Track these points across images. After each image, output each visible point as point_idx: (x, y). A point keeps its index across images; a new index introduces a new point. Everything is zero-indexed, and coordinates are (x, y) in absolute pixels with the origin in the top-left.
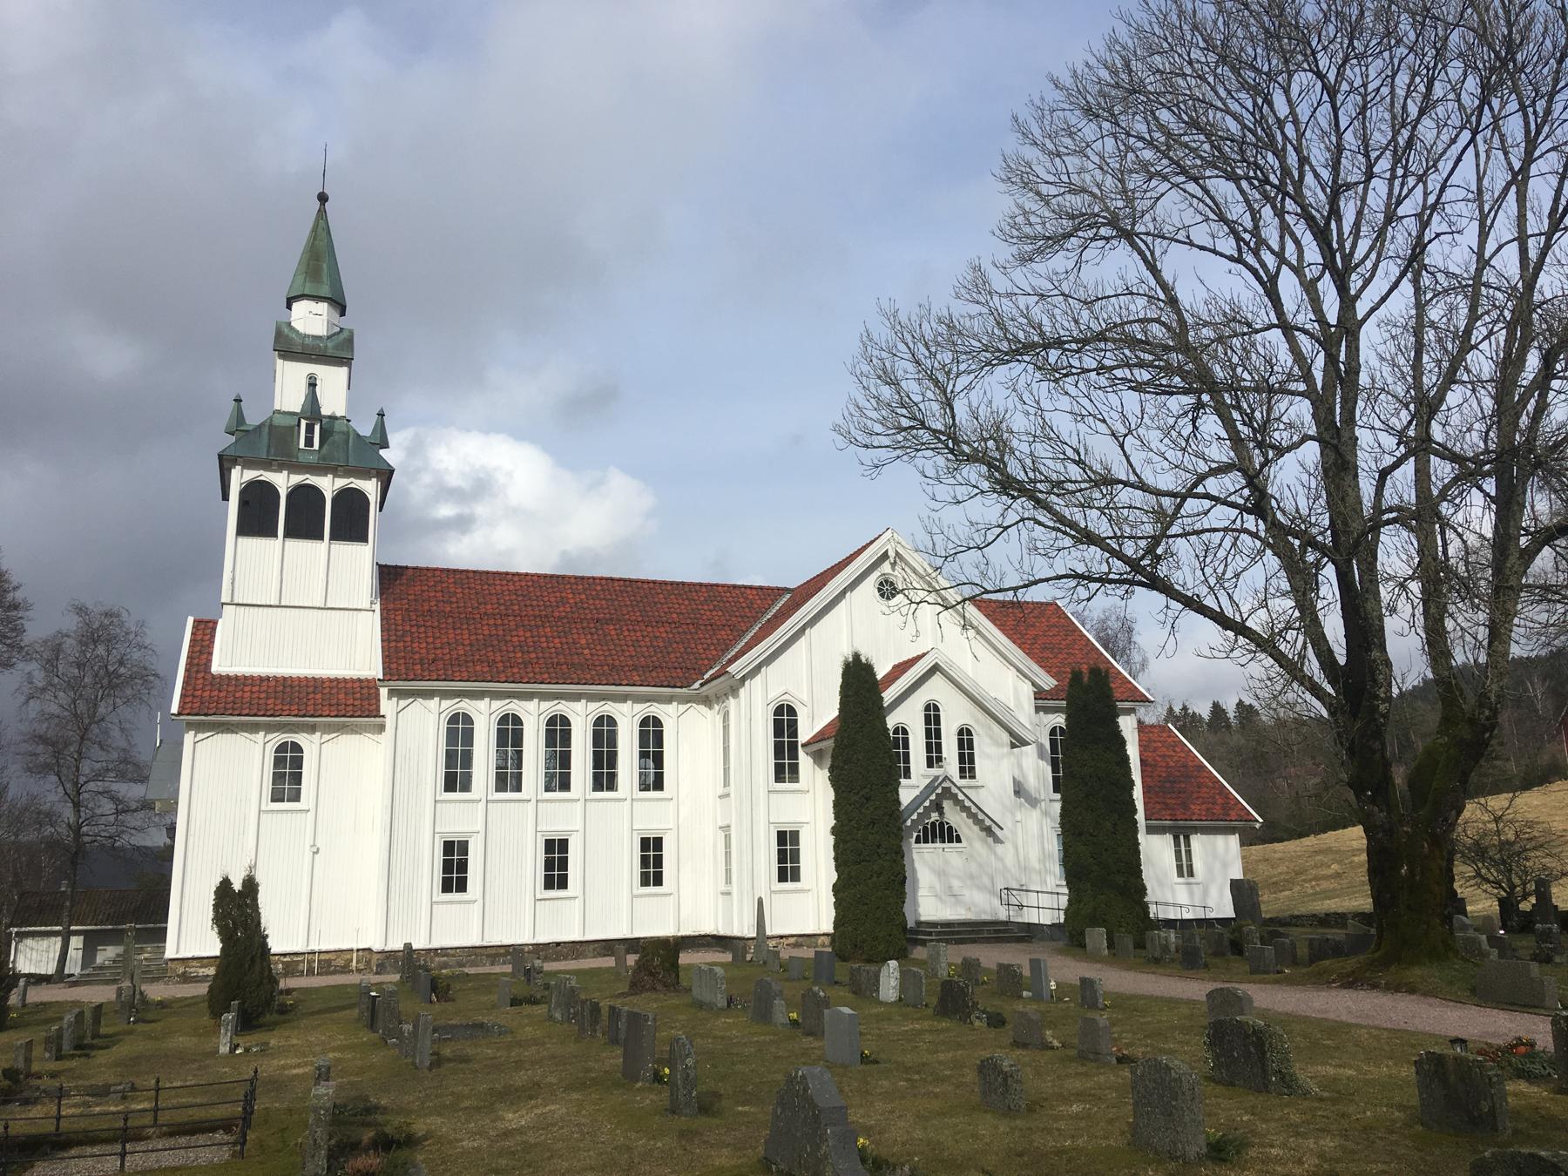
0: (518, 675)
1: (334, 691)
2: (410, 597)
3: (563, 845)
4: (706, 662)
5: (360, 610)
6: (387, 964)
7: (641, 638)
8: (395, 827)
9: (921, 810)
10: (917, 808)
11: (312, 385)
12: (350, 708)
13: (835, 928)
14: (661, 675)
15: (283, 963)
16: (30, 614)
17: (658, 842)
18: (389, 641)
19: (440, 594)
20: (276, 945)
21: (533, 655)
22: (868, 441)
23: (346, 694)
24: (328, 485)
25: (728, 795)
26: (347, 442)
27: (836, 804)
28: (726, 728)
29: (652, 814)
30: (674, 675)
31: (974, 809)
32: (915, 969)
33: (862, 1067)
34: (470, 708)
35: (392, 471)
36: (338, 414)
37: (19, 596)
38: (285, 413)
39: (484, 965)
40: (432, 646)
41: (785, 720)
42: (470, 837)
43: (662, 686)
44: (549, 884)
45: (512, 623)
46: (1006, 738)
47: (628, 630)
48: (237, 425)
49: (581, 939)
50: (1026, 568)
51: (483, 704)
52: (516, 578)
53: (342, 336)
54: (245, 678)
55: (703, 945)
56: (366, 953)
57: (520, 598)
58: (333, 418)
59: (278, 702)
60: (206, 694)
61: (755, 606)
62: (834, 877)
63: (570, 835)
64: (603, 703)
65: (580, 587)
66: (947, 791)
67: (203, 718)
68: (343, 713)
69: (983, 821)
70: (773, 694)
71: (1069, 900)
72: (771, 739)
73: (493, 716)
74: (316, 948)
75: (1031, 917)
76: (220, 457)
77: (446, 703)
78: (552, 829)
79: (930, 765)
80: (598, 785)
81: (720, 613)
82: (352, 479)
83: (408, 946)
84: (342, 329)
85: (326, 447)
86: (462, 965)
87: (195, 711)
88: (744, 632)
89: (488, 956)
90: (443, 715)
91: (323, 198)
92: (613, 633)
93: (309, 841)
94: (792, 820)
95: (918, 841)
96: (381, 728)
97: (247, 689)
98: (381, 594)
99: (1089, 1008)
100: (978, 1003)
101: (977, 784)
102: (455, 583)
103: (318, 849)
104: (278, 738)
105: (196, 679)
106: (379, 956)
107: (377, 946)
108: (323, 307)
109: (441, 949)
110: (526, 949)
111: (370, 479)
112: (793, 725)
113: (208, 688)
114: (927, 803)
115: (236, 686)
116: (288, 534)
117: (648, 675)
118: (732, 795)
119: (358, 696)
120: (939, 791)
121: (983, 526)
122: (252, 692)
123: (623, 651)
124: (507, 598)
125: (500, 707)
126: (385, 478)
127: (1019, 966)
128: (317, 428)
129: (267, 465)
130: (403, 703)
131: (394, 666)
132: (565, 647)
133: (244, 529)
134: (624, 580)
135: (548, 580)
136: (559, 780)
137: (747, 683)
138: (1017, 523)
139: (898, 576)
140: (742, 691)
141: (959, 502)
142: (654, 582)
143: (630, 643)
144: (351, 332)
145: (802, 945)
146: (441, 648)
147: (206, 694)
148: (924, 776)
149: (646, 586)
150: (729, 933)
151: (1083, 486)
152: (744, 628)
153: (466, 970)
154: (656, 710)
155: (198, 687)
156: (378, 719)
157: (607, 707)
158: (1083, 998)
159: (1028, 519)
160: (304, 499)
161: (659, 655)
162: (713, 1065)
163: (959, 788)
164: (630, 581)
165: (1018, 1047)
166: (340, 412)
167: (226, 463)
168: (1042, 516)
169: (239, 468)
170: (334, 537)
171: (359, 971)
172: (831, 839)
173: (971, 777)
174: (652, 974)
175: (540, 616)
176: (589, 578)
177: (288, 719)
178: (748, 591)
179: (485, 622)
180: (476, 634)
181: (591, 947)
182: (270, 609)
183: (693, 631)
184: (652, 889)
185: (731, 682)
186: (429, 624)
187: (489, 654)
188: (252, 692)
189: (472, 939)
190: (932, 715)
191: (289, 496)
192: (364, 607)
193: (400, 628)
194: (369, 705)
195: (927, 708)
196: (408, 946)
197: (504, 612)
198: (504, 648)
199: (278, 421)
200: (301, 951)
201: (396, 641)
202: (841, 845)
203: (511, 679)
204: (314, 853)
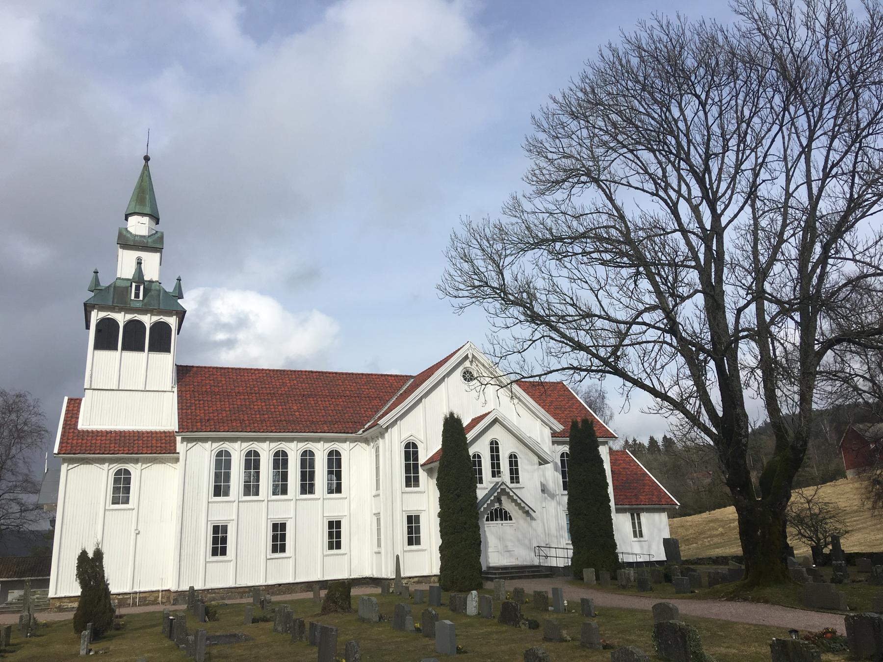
0: (257, 428)
1: (150, 439)
2: (195, 384)
3: (283, 526)
4: (366, 418)
5: (165, 391)
6: (179, 599)
7: (328, 405)
8: (185, 518)
9: (489, 502)
11: (139, 263)
12: (159, 448)
13: (441, 572)
14: (340, 426)
15: (118, 599)
17: (338, 523)
18: (182, 409)
19: (212, 381)
20: (114, 589)
21: (266, 416)
22: (455, 293)
24: (148, 320)
25: (378, 495)
26: (159, 295)
27: (441, 500)
28: (377, 456)
29: (335, 507)
30: (348, 426)
31: (519, 501)
33: (458, 656)
34: (229, 447)
35: (185, 312)
36: (154, 280)
38: (123, 279)
39: (237, 598)
41: (411, 451)
42: (229, 523)
43: (340, 433)
44: (275, 550)
45: (254, 398)
47: (322, 401)
48: (95, 286)
49: (293, 582)
50: (546, 364)
51: (237, 445)
53: (157, 236)
54: (97, 432)
55: (364, 584)
57: (259, 384)
58: (151, 282)
60: (75, 442)
61: (394, 386)
62: (440, 542)
63: (287, 521)
64: (306, 443)
66: (503, 490)
68: (155, 451)
70: (403, 438)
72: (403, 462)
74: (138, 590)
75: (553, 563)
76: (85, 304)
77: (215, 445)
78: (277, 517)
79: (494, 475)
80: (304, 491)
81: (374, 391)
82: (162, 317)
83: (192, 588)
84: (157, 232)
85: (147, 298)
86: (223, 598)
88: (387, 401)
89: (239, 593)
90: (213, 452)
91: (147, 159)
92: (312, 402)
93: (134, 527)
95: (487, 520)
96: (177, 460)
98: (178, 382)
99: (587, 616)
100: (523, 615)
101: (520, 486)
102: (221, 375)
103: (139, 531)
104: (116, 467)
107: (173, 588)
108: (146, 219)
109: (212, 589)
110: (261, 588)
111: (172, 316)
112: (416, 454)
114: (492, 498)
115: (92, 437)
119: (164, 441)
121: (520, 340)
123: (318, 413)
125: (247, 446)
126: (181, 316)
127: (546, 592)
128: (142, 288)
129: (112, 309)
130: (190, 445)
131: (184, 424)
132: (285, 411)
133: (98, 346)
134: (319, 372)
135: (275, 372)
136: (281, 488)
137: (389, 430)
138: (540, 338)
139: (474, 369)
140: (386, 435)
141: (508, 327)
142: (336, 373)
145: (421, 582)
146: (213, 413)
147: (75, 442)
149: (331, 375)
150: (379, 576)
151: (576, 318)
152: (387, 399)
153: (227, 602)
154: (338, 447)
155: (70, 438)
156: (175, 455)
159: (546, 336)
160: (133, 328)
161: (339, 415)
163: (510, 489)
164: (322, 373)
165: (547, 641)
166: (155, 278)
167: (88, 308)
168: (554, 335)
169: (96, 311)
171: (163, 603)
172: (438, 520)
173: (516, 483)
174: (335, 602)
175: (270, 394)
176: (299, 371)
178: (390, 378)
180: (233, 404)
181: (300, 586)
182: (113, 392)
183: (358, 401)
184: (335, 551)
185: (379, 430)
186: (206, 399)
187: (240, 416)
189: (230, 584)
190: (494, 447)
191: (125, 327)
192: (167, 390)
194: (170, 446)
195: (492, 443)
196: (192, 588)
198: (249, 412)
199: (119, 283)
201: (186, 409)
202: (444, 524)
203: (254, 430)
204: (137, 534)
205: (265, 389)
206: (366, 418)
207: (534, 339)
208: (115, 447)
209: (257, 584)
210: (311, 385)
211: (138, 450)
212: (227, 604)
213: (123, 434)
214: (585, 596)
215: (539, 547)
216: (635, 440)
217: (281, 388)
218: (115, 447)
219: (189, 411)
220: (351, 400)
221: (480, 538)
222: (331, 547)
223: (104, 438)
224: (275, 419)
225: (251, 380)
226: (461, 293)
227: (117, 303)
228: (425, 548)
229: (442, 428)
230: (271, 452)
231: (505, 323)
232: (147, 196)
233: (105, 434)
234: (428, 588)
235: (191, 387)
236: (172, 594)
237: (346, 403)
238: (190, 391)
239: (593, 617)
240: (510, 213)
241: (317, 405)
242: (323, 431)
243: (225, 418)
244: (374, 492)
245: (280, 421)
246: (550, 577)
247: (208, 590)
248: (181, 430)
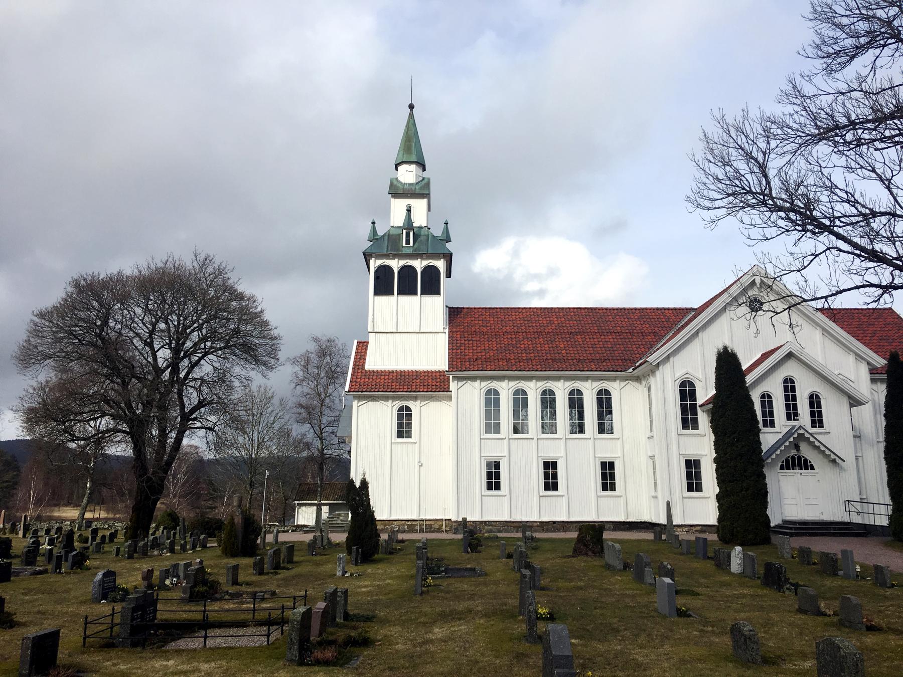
1: (427, 377)
2: (465, 325)
3: (554, 465)
4: (638, 356)
5: (438, 333)
6: (459, 529)
7: (597, 343)
8: (460, 453)
9: (783, 448)
10: (779, 447)
11: (409, 210)
12: (434, 387)
13: (718, 522)
14: (609, 364)
15: (407, 525)
16: (282, 342)
18: (453, 349)
19: (481, 322)
20: (379, 516)
21: (532, 355)
22: (708, 204)
23: (432, 379)
24: (419, 265)
25: (652, 437)
27: (716, 443)
28: (650, 396)
30: (617, 364)
31: (822, 448)
32: (750, 553)
33: (677, 619)
35: (451, 255)
36: (423, 226)
37: (275, 333)
38: (396, 227)
40: (475, 351)
41: (687, 391)
43: (609, 371)
44: (547, 487)
46: (845, 402)
47: (590, 338)
48: (374, 237)
52: (524, 311)
55: (643, 528)
56: (450, 522)
58: (421, 228)
59: (397, 384)
60: (362, 381)
62: (717, 490)
64: (573, 382)
65: (561, 314)
66: (801, 436)
67: (360, 393)
68: (430, 390)
69: (829, 456)
71: (893, 510)
72: (679, 402)
73: (510, 391)
74: (424, 518)
75: (869, 520)
76: (364, 254)
77: (484, 384)
78: (547, 455)
79: (789, 418)
81: (648, 326)
83: (464, 519)
84: (424, 178)
85: (417, 244)
86: (500, 531)
87: (357, 390)
88: (663, 336)
89: (514, 527)
90: (482, 390)
91: (411, 107)
92: (580, 340)
93: (417, 460)
94: (695, 453)
96: (450, 398)
97: (382, 377)
98: (449, 324)
99: (881, 585)
100: (789, 579)
101: (826, 431)
103: (422, 464)
104: (399, 404)
105: (358, 372)
106: (454, 524)
107: (453, 519)
109: (488, 522)
110: (536, 524)
111: (440, 259)
112: (693, 394)
113: (363, 377)
114: (787, 444)
116: (399, 293)
117: (600, 364)
118: (655, 437)
119: (439, 380)
120: (796, 435)
121: (800, 256)
122: (385, 379)
123: (586, 350)
124: (519, 322)
126: (449, 258)
127: (835, 554)
128: (411, 234)
129: (386, 256)
130: (460, 384)
131: (455, 363)
132: (551, 349)
133: (377, 293)
134: (588, 309)
135: (542, 311)
136: (549, 425)
137: (661, 368)
138: (825, 251)
139: (764, 296)
140: (657, 373)
142: (606, 309)
143: (590, 346)
144: (429, 179)
145: (704, 532)
147: (362, 381)
148: (786, 426)
149: (601, 311)
150: (657, 522)
151: (854, 220)
153: (500, 535)
156: (448, 393)
157: (576, 384)
158: (877, 578)
159: (832, 248)
160: (407, 273)
162: (581, 608)
163: (811, 434)
164: (592, 309)
166: (424, 224)
167: (367, 256)
169: (373, 259)
170: (422, 294)
171: (446, 531)
172: (714, 466)
173: (819, 427)
174: (585, 545)
176: (566, 309)
177: (374, 393)
178: (667, 311)
179: (505, 337)
180: (500, 344)
183: (630, 337)
184: (609, 493)
185: (650, 367)
188: (385, 379)
189: (505, 518)
190: (789, 386)
191: (399, 273)
193: (459, 342)
194: (444, 385)
195: (786, 381)
196: (464, 519)
197: (516, 331)
198: (516, 351)
199: (393, 232)
200: (416, 519)
202: (720, 470)
203: (519, 369)
205: (531, 328)
206: (638, 356)
207: (816, 253)
208: (396, 386)
209: (532, 520)
210: (579, 322)
211: (416, 388)
212: (497, 537)
213: (403, 374)
214: (882, 561)
215: (848, 501)
216: (262, 312)
217: (548, 326)
218: (396, 386)
219: (459, 351)
220: (622, 337)
221: (767, 488)
222: (489, 487)
223: (387, 377)
224: (541, 358)
225: (519, 319)
226: (718, 204)
227: (391, 250)
228: (708, 496)
229: (715, 364)
230: (538, 390)
231: (762, 234)
232: (413, 144)
233: (388, 374)
234: (694, 539)
235: (461, 327)
236: (454, 524)
237: (616, 340)
238: (459, 331)
239: (889, 588)
240: (787, 101)
241: (585, 342)
242: (590, 369)
243: (492, 358)
244: (649, 434)
245: (546, 359)
246: (863, 536)
247: (486, 522)
248: (451, 369)
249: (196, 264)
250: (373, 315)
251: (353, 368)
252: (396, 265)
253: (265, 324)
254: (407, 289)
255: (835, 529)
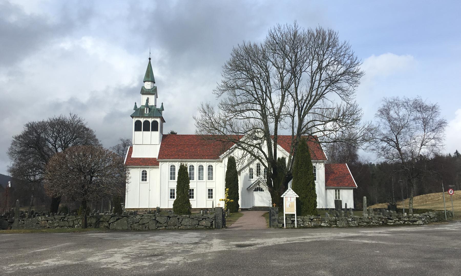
17: (212, 190)
18: (161, 151)
21: (188, 153)
24: (151, 120)
37: (100, 143)
58: (152, 106)
74: (150, 208)
77: (170, 163)
84: (154, 87)
91: (150, 59)
95: (254, 191)
96: (158, 168)
104: (142, 170)
108: (150, 83)
129: (139, 117)
130: (162, 163)
144: (156, 87)
160: (147, 123)
169: (134, 118)
170: (152, 131)
181: (198, 209)
184: (210, 199)
191: (144, 123)
199: (143, 108)
249: (71, 118)
250: (134, 138)
251: (127, 157)
252: (142, 120)
253: (97, 140)
254: (146, 129)
255: (263, 209)
